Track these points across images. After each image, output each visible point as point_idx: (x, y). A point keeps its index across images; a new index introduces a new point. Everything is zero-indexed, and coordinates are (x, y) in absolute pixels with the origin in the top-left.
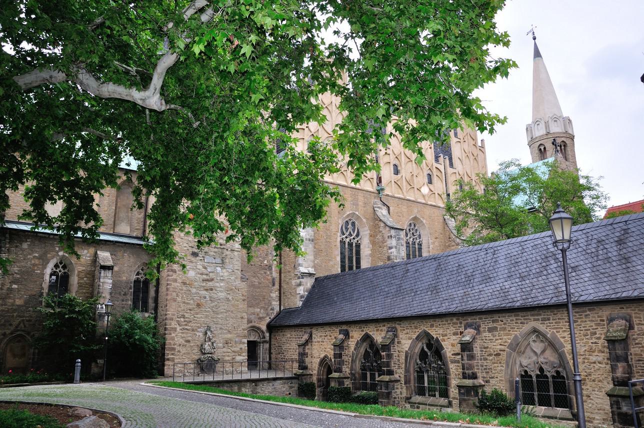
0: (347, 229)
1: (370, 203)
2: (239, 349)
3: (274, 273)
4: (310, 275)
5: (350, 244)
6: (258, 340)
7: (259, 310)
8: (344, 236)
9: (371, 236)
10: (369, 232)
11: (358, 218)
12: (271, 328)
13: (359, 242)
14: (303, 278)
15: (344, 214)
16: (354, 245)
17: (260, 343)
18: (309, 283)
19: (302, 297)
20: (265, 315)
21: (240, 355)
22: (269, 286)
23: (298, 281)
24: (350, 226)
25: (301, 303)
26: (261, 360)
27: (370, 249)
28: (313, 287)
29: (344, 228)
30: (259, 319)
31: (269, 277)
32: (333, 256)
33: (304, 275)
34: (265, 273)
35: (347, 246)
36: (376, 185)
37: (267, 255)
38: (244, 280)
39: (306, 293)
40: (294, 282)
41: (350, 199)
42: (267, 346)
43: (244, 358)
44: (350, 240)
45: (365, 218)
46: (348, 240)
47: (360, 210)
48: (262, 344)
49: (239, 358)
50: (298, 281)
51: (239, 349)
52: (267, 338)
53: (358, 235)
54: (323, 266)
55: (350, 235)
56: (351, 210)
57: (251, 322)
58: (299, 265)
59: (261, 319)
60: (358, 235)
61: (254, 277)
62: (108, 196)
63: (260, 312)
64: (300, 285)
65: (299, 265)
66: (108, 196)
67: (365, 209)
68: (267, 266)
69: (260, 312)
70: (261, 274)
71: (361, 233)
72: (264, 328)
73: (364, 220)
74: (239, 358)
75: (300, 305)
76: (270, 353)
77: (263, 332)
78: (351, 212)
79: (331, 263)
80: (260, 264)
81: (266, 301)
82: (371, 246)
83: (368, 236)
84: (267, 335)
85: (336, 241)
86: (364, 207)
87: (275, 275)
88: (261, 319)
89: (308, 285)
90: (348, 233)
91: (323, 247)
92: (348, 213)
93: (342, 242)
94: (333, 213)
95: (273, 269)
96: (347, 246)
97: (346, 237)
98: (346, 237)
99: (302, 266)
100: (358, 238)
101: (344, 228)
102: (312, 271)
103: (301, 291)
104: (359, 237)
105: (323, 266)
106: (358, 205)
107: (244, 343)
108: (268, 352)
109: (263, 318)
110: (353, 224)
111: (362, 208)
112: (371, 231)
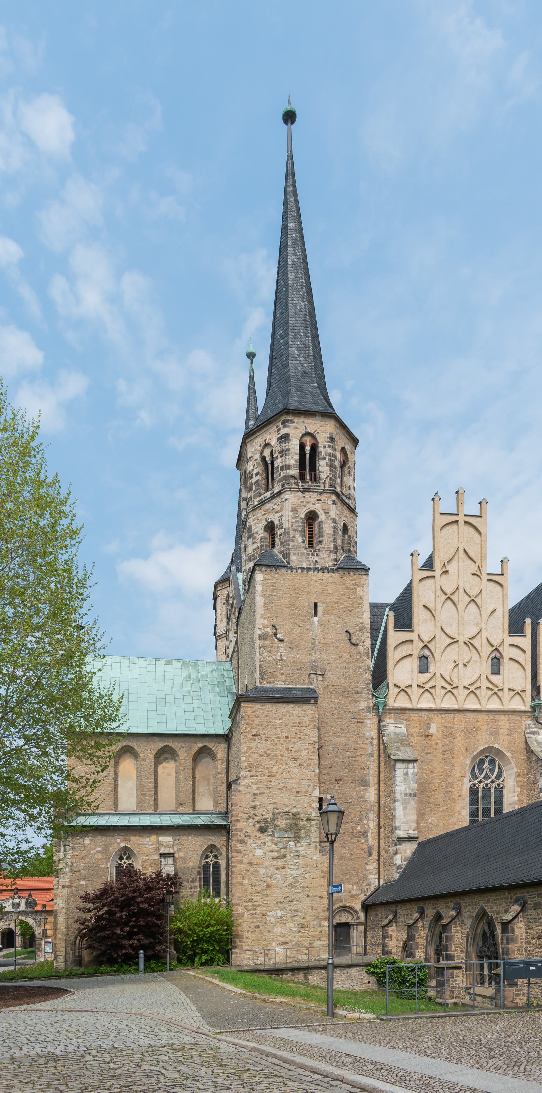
0: (481, 770)
1: (519, 727)
2: (317, 933)
3: (370, 840)
4: (410, 839)
5: (486, 790)
6: (352, 921)
7: (351, 886)
8: (476, 781)
9: (519, 775)
10: (515, 770)
11: (499, 752)
12: (367, 907)
13: (501, 786)
14: (400, 845)
15: (476, 749)
16: (492, 790)
17: (353, 925)
18: (409, 849)
19: (398, 868)
20: (358, 892)
21: (319, 940)
22: (363, 857)
23: (394, 848)
24: (486, 765)
25: (398, 875)
26: (355, 944)
27: (516, 794)
28: (414, 854)
29: (476, 769)
30: (351, 897)
31: (364, 846)
32: (456, 810)
33: (401, 840)
34: (358, 841)
35: (480, 794)
36: (530, 699)
37: (360, 819)
38: (324, 853)
39: (405, 863)
40: (392, 849)
41: (486, 727)
42: (362, 928)
43: (325, 943)
44: (487, 785)
45: (510, 751)
46: (482, 785)
47: (502, 739)
48: (355, 927)
49: (318, 943)
50: (394, 848)
51: (317, 933)
52: (362, 919)
53: (499, 777)
54: (441, 825)
55: (487, 777)
56: (487, 743)
57: (341, 901)
58: (396, 828)
59: (354, 897)
60: (499, 777)
61: (344, 847)
62: (184, 770)
63: (353, 888)
64: (396, 853)
65: (396, 828)
66: (184, 770)
67: (510, 738)
68: (360, 832)
69: (353, 888)
70: (354, 843)
71: (505, 774)
72: (358, 907)
73: (508, 754)
74: (318, 943)
75: (397, 878)
76: (366, 937)
77: (356, 912)
78: (486, 746)
79: (453, 819)
80: (351, 830)
81: (361, 875)
82: (518, 789)
83: (514, 776)
84: (362, 915)
85: (461, 790)
86: (509, 735)
87: (372, 842)
88: (354, 897)
89: (408, 852)
90: (482, 776)
91: (440, 800)
92: (481, 748)
93: (473, 792)
94: (456, 752)
95: (370, 836)
96: (480, 794)
97: (480, 782)
98: (480, 782)
99: (400, 829)
100: (500, 781)
101: (476, 769)
102: (413, 833)
103: (398, 860)
104: (502, 779)
105: (441, 825)
106: (497, 733)
107: (323, 926)
108: (363, 934)
109: (356, 895)
110: (492, 762)
111: (506, 738)
112: (518, 768)
